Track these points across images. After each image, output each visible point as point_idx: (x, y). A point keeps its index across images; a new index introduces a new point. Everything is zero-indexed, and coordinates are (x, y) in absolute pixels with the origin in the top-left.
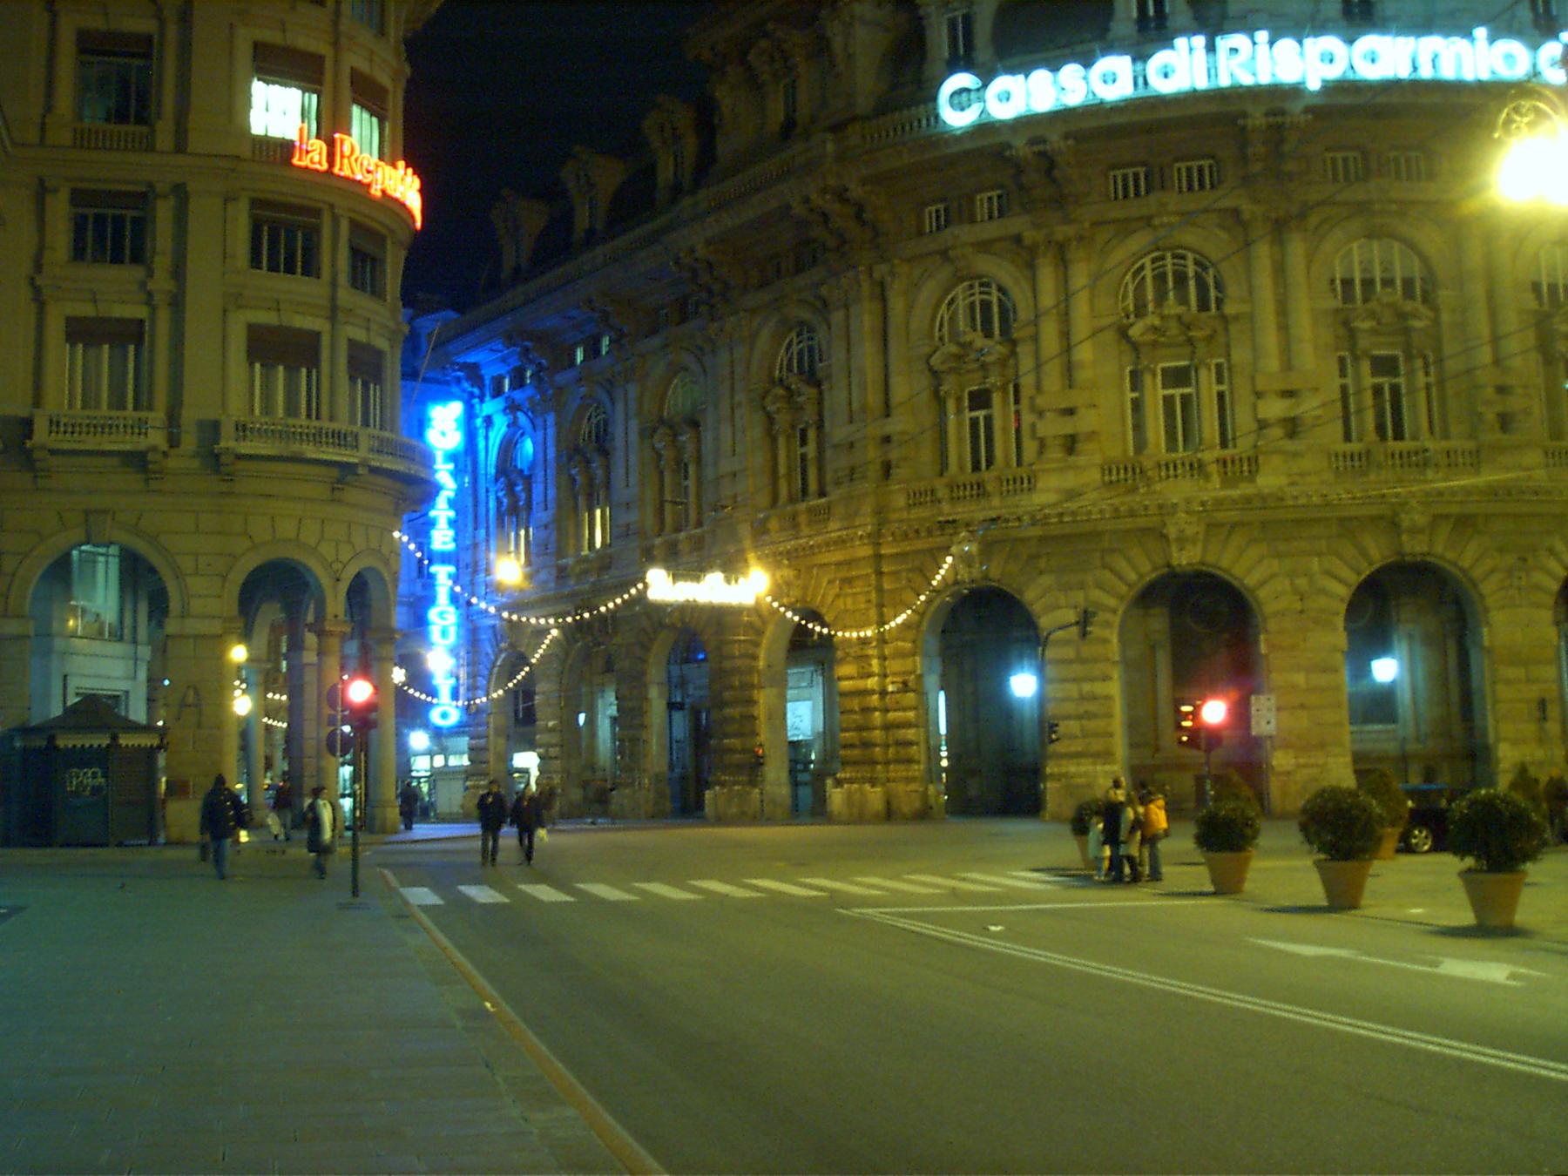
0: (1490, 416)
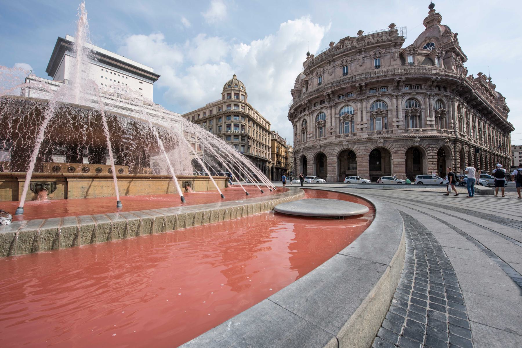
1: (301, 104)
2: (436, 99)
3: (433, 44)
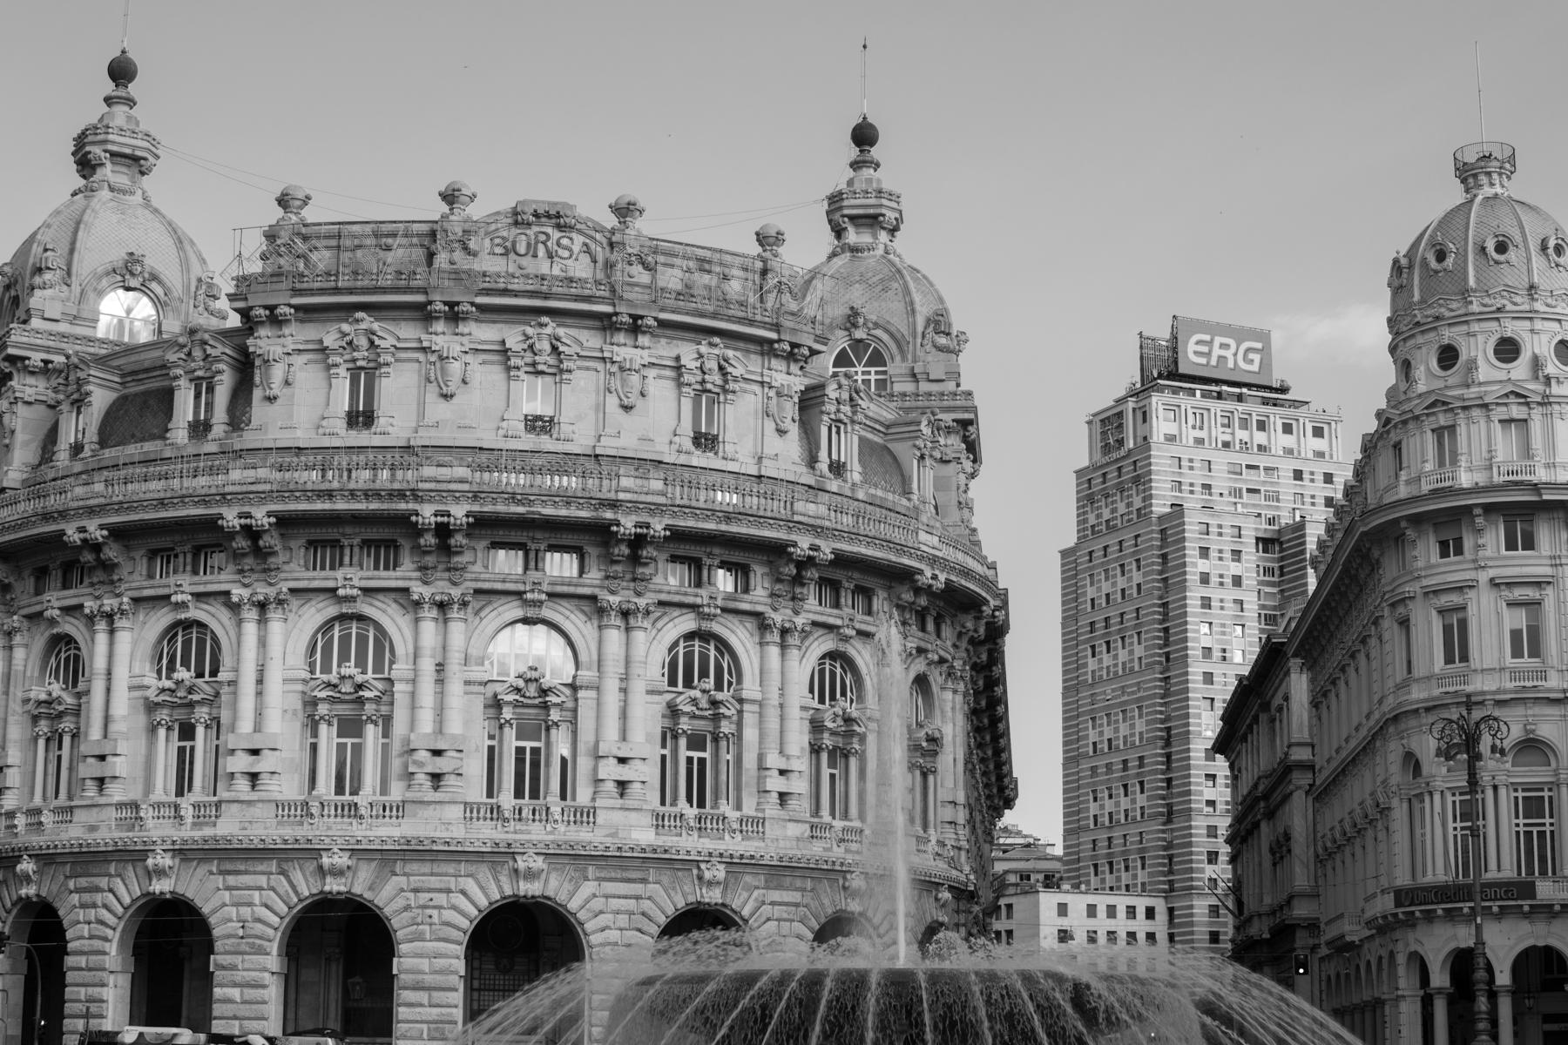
0: (421, 778)
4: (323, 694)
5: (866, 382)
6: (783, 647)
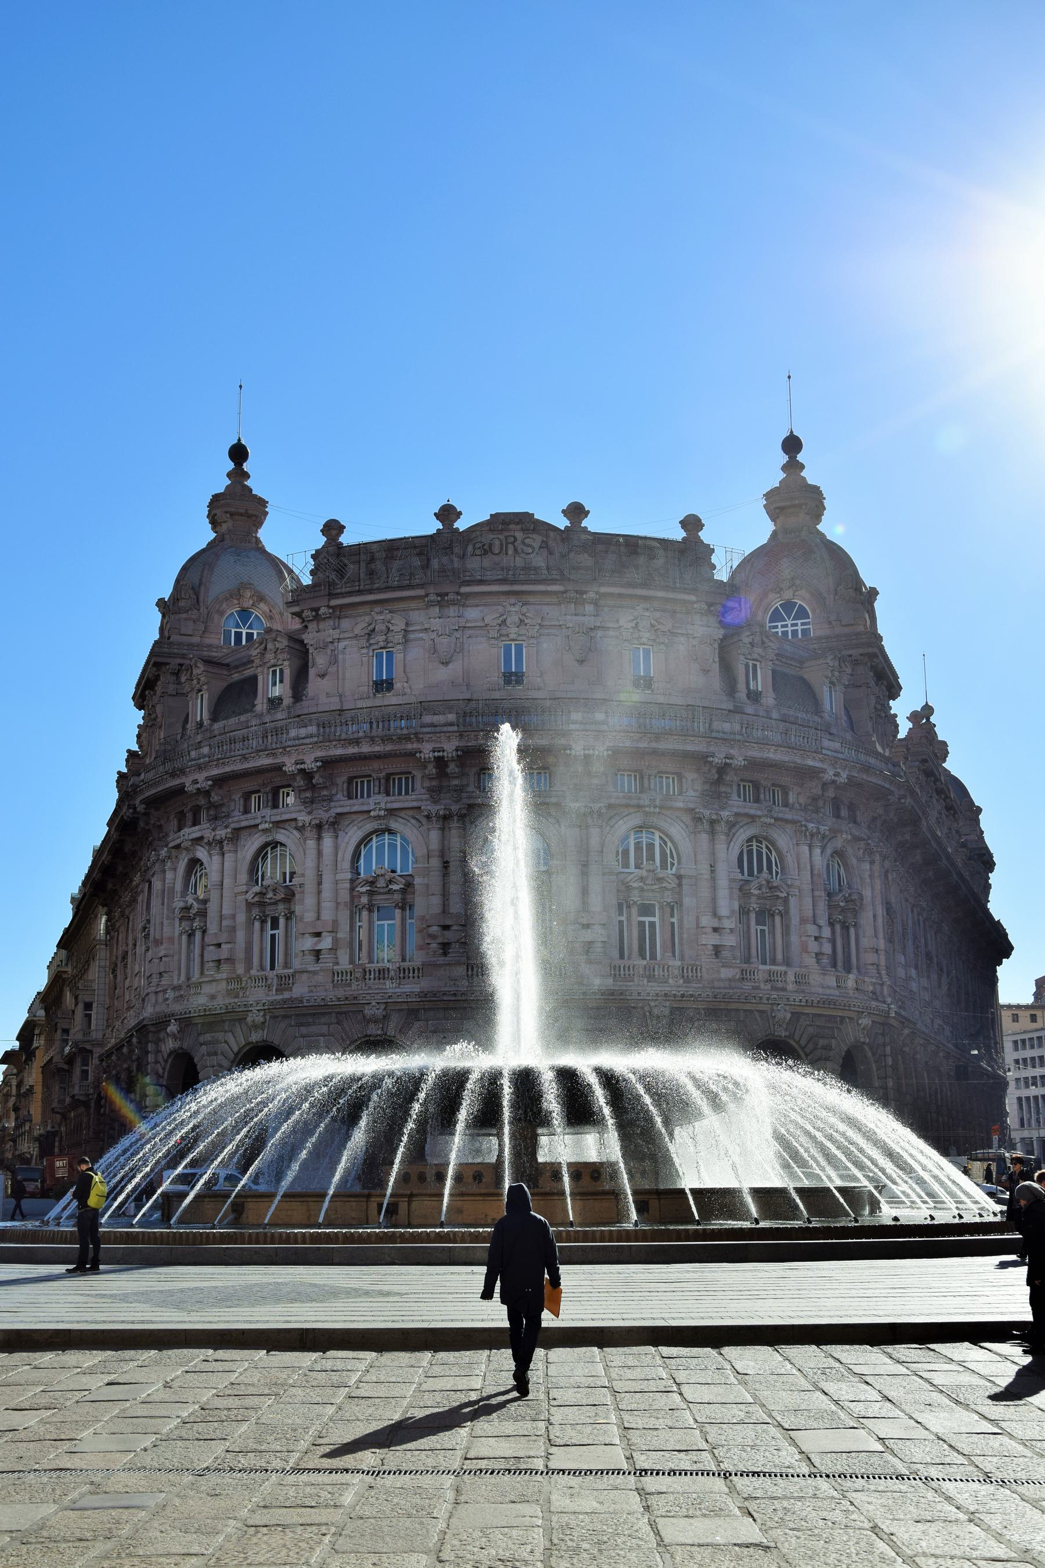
0: (434, 945)
1: (278, 768)
2: (829, 851)
3: (802, 613)
4: (364, 889)
5: (795, 633)
6: (712, 833)
